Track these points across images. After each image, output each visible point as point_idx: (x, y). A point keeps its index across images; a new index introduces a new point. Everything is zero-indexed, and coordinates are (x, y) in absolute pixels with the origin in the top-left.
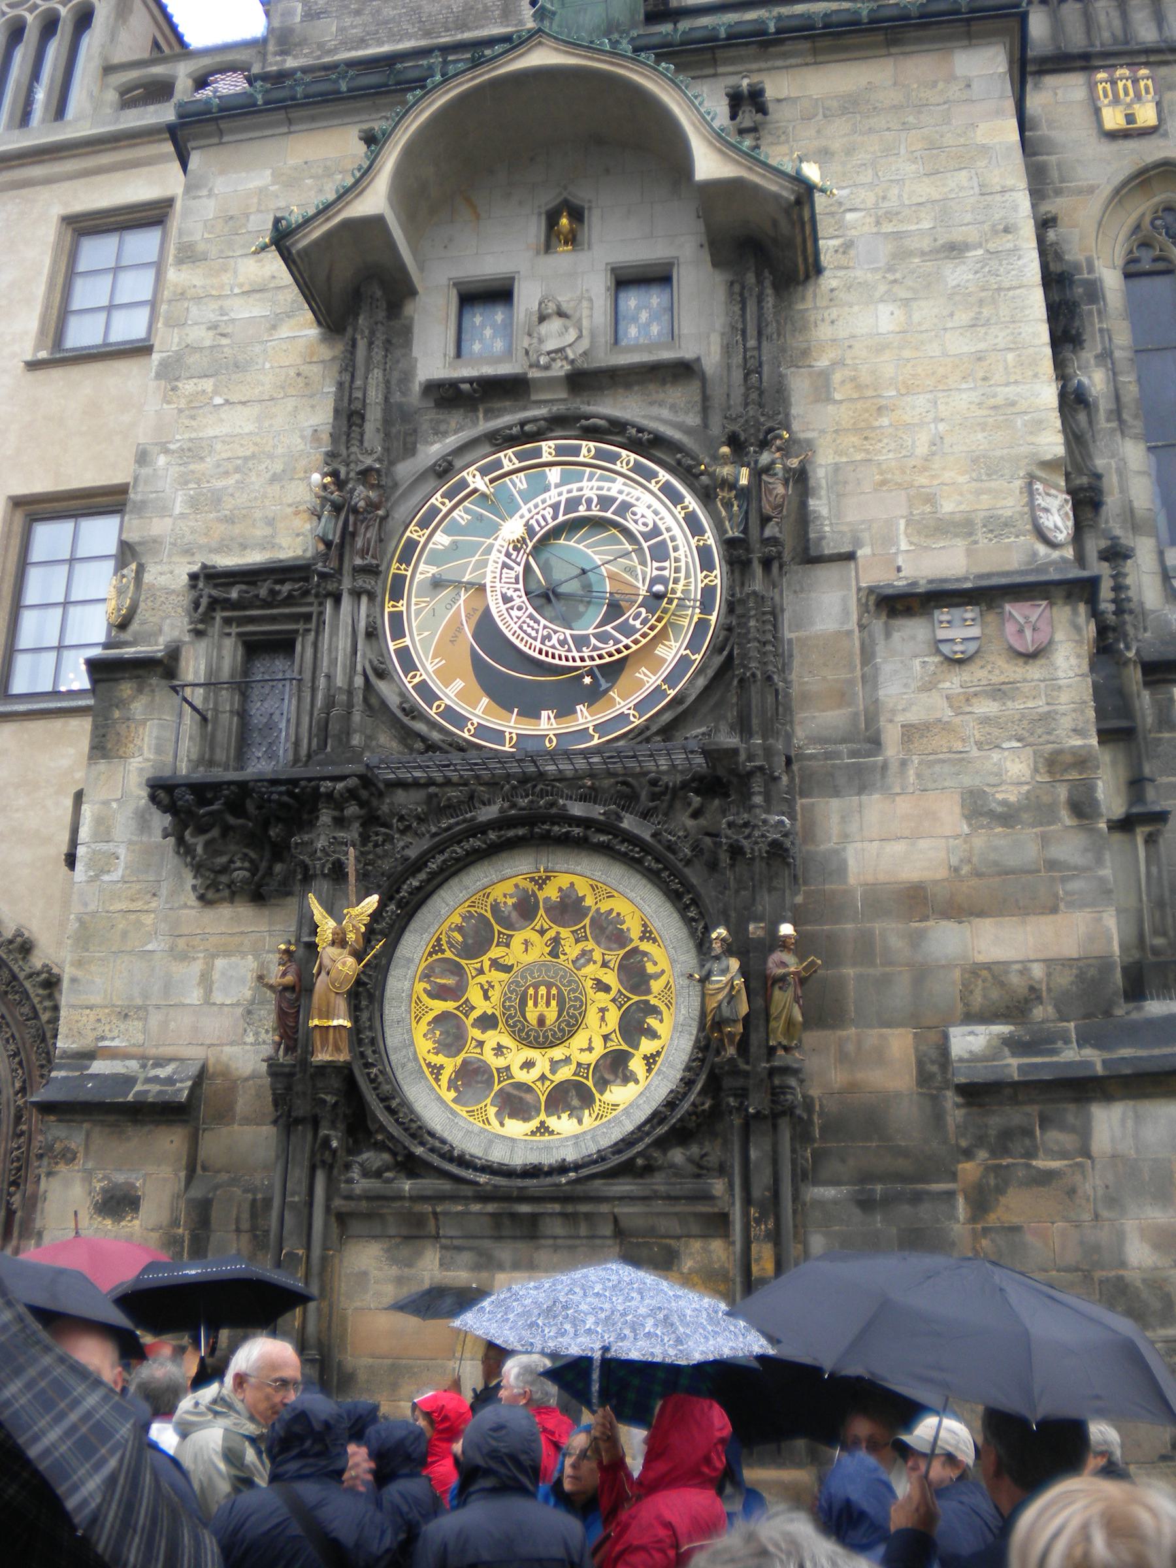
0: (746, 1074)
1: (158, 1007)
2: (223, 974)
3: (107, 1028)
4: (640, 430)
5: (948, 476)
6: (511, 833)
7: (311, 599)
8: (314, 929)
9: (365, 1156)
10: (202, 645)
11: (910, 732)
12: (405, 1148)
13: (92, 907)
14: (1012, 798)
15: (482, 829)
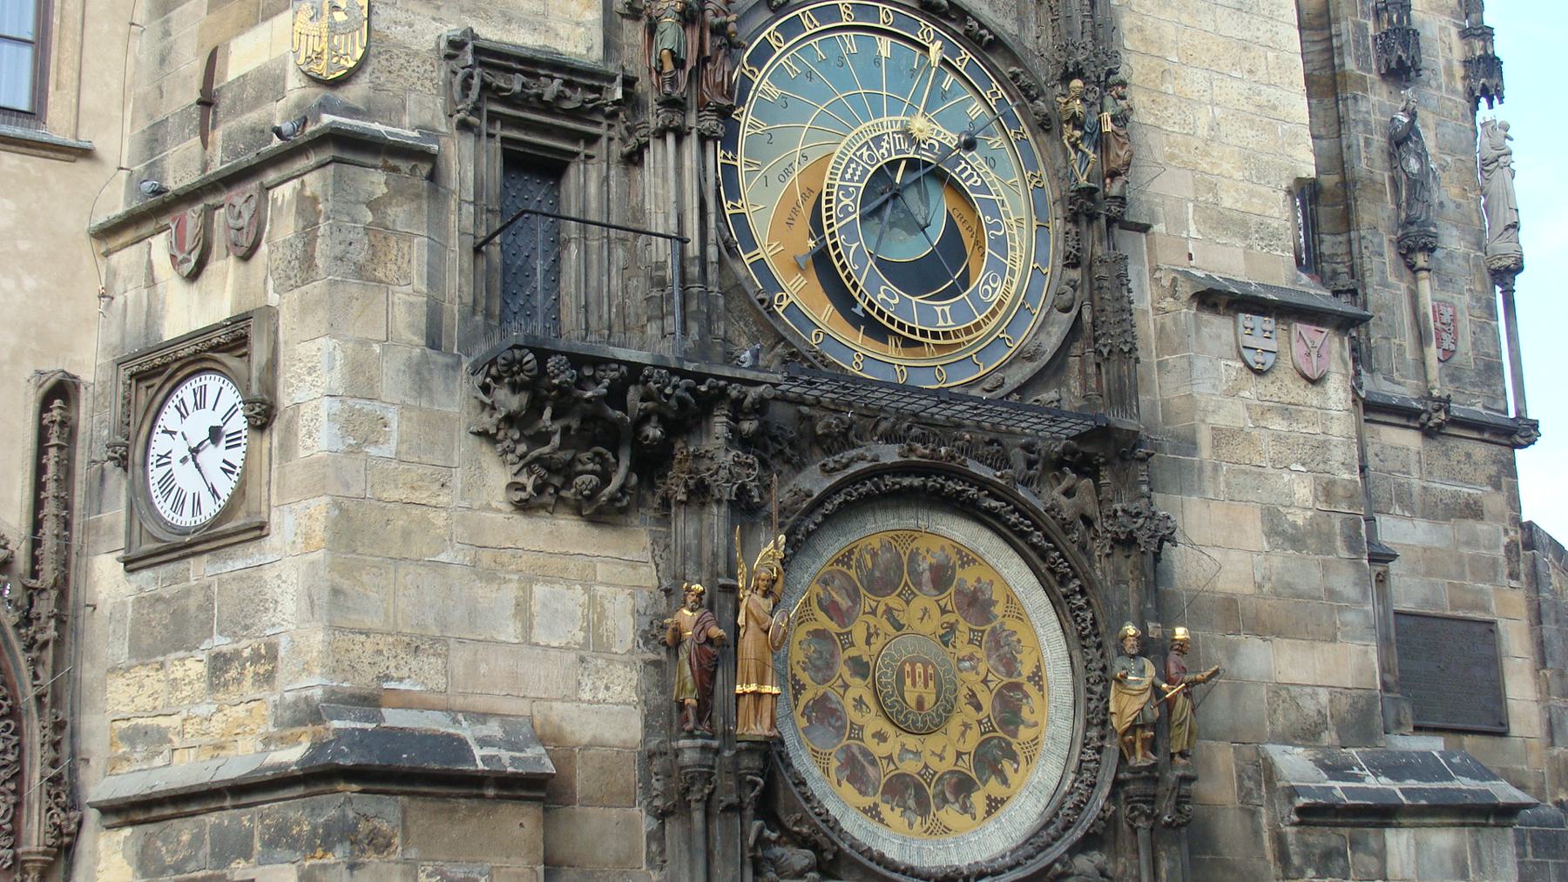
0: (1156, 781)
1: (461, 641)
2: (545, 605)
3: (392, 664)
4: (982, 26)
5: (1226, 167)
6: (906, 482)
7: (600, 118)
8: (732, 574)
9: (778, 851)
10: (468, 142)
11: (1221, 436)
12: (833, 843)
13: (356, 490)
14: (1300, 522)
15: (879, 472)
